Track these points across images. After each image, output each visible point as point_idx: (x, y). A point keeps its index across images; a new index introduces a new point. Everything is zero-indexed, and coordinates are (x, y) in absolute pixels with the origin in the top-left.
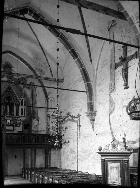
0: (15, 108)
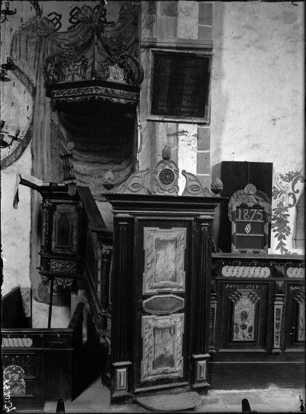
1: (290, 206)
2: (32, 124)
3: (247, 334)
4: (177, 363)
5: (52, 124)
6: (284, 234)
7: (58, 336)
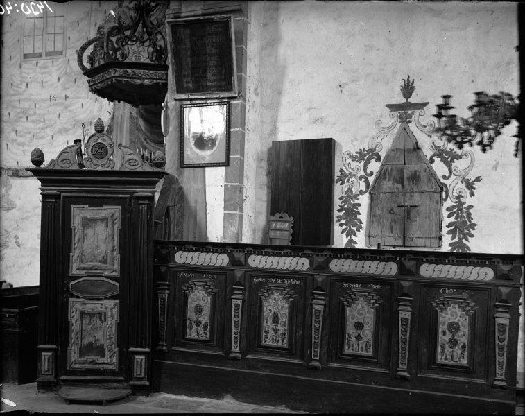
1: (362, 193)
2: (113, 118)
3: (202, 332)
4: (108, 354)
5: (131, 117)
6: (355, 229)
7: (7, 316)
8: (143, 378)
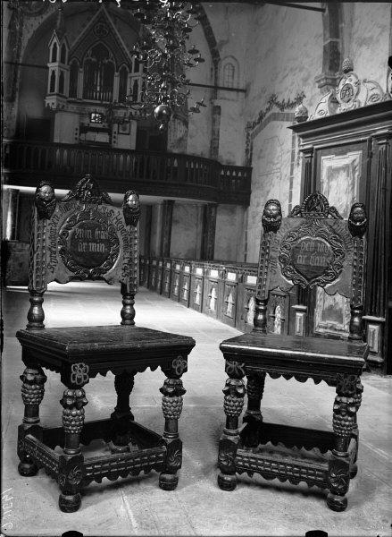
0: (116, 81)
8: (375, 353)
